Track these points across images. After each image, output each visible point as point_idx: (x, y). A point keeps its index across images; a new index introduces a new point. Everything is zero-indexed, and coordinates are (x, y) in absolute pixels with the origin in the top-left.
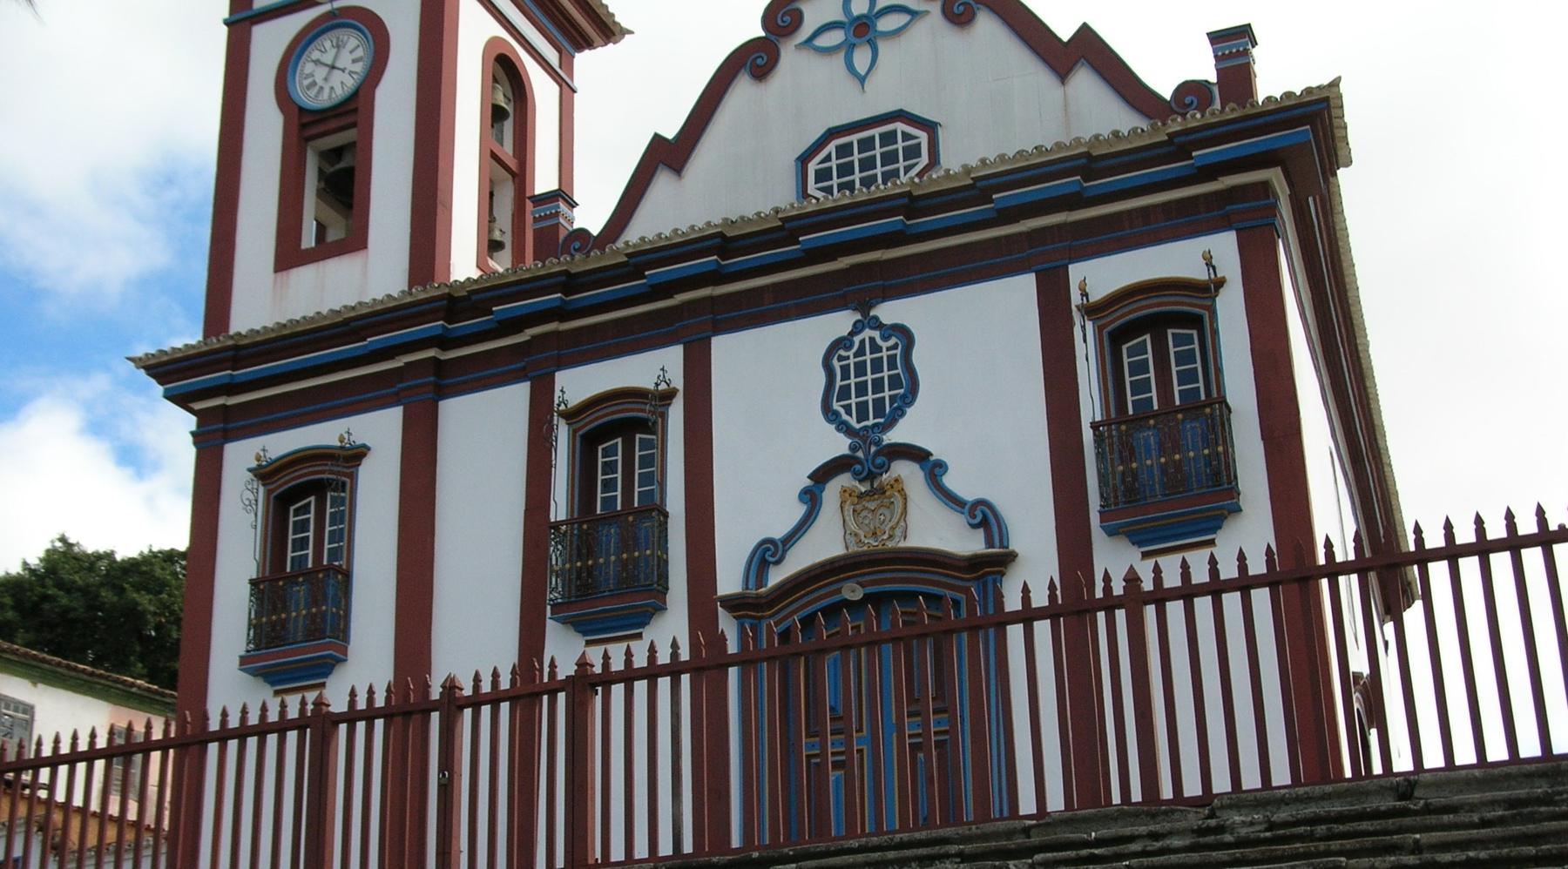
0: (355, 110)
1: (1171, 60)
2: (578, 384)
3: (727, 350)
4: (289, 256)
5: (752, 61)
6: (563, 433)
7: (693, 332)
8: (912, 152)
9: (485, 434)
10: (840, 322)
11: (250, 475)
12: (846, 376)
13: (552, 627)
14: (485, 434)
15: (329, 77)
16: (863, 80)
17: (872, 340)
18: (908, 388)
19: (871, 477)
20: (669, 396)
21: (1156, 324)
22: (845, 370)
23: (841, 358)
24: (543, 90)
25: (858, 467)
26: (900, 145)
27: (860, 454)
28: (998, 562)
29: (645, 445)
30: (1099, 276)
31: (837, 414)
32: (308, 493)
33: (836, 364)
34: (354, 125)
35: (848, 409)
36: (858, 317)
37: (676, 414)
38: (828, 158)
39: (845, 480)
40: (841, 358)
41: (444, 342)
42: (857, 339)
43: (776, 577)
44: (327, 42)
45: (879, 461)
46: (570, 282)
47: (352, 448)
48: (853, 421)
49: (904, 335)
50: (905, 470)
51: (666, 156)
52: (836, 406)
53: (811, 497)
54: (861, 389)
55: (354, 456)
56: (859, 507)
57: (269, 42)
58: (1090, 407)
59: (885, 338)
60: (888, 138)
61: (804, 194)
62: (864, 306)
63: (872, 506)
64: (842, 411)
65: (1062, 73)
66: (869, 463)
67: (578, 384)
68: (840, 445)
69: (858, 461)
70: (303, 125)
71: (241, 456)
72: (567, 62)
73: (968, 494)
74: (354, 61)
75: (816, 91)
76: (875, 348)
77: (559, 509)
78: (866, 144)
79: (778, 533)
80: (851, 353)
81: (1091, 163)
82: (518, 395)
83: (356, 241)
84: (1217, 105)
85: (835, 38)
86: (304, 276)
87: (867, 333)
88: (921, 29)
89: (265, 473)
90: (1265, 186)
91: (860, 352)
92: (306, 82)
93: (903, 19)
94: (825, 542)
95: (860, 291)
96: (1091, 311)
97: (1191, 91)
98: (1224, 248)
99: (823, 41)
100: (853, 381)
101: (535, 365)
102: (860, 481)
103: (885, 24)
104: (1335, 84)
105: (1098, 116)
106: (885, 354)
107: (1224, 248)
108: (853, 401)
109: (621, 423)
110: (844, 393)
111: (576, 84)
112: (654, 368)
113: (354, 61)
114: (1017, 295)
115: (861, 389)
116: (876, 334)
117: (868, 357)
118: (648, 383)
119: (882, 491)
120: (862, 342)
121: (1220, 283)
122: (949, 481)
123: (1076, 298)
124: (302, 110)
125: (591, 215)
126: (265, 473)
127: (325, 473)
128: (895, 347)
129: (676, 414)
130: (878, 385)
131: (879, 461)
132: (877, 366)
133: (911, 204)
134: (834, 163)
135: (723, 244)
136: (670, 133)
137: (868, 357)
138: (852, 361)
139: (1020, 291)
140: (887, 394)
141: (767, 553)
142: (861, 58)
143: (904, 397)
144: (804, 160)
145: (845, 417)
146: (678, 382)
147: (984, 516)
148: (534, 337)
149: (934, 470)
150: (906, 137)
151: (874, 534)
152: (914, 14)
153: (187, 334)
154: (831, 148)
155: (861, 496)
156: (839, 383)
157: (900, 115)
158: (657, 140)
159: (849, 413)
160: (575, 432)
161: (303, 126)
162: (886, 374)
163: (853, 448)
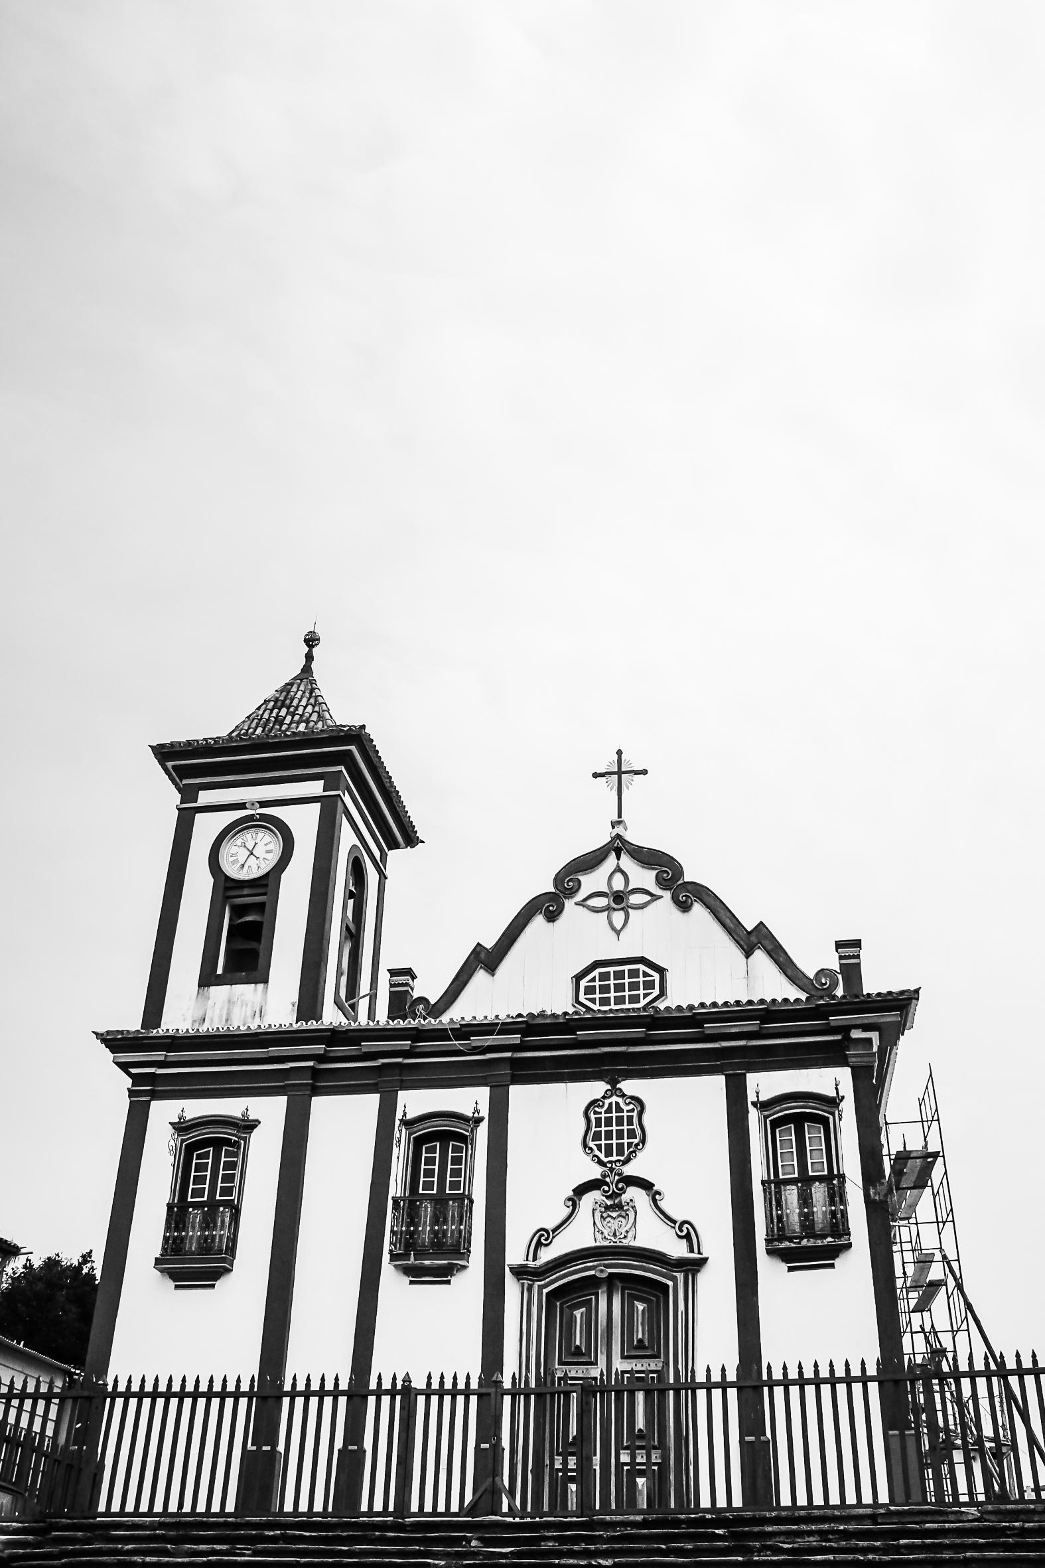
0: (268, 884)
1: (816, 956)
4: (208, 979)
5: (547, 906)
6: (401, 1135)
8: (649, 985)
10: (598, 1088)
11: (170, 1130)
12: (598, 1124)
15: (250, 857)
16: (618, 933)
17: (617, 1103)
20: (479, 1121)
22: (598, 1120)
23: (596, 1113)
25: (606, 1188)
26: (641, 979)
27: (607, 1179)
29: (457, 1149)
30: (765, 1084)
31: (591, 1149)
33: (593, 1117)
34: (265, 894)
35: (599, 1147)
36: (609, 1087)
37: (482, 1132)
38: (593, 980)
39: (595, 1196)
40: (596, 1113)
42: (607, 1102)
45: (620, 1185)
46: (418, 1035)
47: (248, 1120)
48: (602, 1156)
49: (638, 1101)
51: (487, 959)
52: (591, 1144)
54: (609, 1135)
55: (249, 1126)
56: (605, 1215)
57: (207, 828)
58: (758, 1172)
59: (628, 1104)
60: (634, 974)
62: (613, 1083)
63: (614, 1214)
64: (595, 1148)
66: (613, 1187)
67: (415, 1102)
68: (596, 1172)
69: (607, 1184)
73: (679, 1218)
74: (268, 852)
76: (619, 1109)
78: (619, 975)
79: (550, 1226)
80: (603, 1110)
86: (219, 993)
87: (614, 1099)
90: (869, 1041)
91: (609, 1110)
92: (231, 859)
93: (647, 898)
95: (610, 1067)
99: (591, 902)
100: (603, 1129)
101: (385, 1080)
102: (607, 1197)
103: (635, 899)
104: (917, 991)
106: (625, 1114)
108: (603, 1142)
109: (444, 1134)
110: (597, 1136)
111: (387, 873)
112: (470, 1100)
113: (268, 852)
114: (710, 1089)
115: (609, 1135)
116: (620, 1100)
117: (614, 1115)
119: (620, 1207)
120: (611, 1104)
123: (751, 1097)
124: (227, 878)
125: (429, 987)
128: (632, 1110)
129: (482, 1132)
130: (620, 1135)
131: (620, 1185)
132: (620, 1121)
134: (597, 983)
136: (489, 944)
137: (614, 1115)
138: (603, 1116)
139: (716, 1084)
140: (626, 1141)
141: (542, 1238)
143: (637, 1145)
144: (578, 978)
145: (597, 1153)
146: (484, 1112)
148: (384, 1064)
150: (645, 974)
151: (615, 1235)
154: (596, 973)
155: (607, 1208)
156: (594, 1129)
157: (642, 960)
158: (479, 944)
159: (600, 1150)
160: (410, 1135)
161: (227, 889)
162: (625, 1127)
163: (604, 1176)
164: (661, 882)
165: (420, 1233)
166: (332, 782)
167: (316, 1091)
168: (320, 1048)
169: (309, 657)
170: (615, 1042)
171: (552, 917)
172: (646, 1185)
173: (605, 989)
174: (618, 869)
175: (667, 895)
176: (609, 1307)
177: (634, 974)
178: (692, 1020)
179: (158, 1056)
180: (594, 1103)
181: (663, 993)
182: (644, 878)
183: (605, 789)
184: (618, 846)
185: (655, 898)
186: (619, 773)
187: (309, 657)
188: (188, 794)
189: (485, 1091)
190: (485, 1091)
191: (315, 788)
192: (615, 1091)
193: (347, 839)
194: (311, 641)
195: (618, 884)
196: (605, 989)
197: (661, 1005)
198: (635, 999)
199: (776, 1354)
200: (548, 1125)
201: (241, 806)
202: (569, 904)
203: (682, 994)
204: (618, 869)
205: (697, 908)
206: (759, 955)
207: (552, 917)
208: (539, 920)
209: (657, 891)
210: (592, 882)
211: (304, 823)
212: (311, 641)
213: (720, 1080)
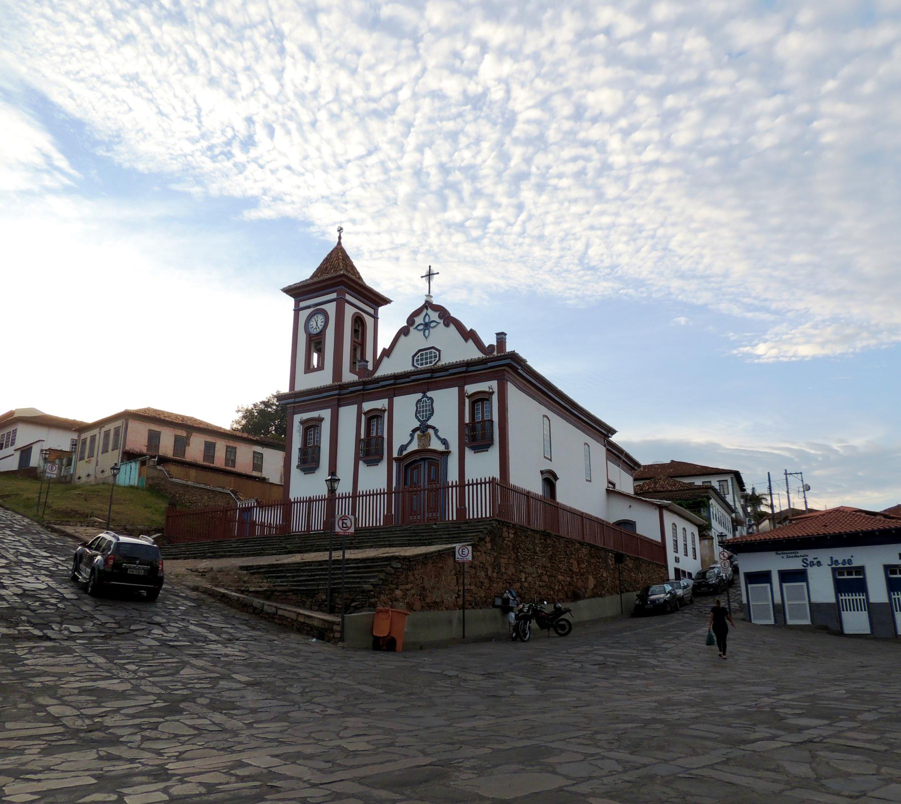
0: (322, 333)
3: (396, 399)
4: (308, 368)
5: (404, 332)
8: (435, 356)
9: (348, 415)
10: (419, 396)
13: (361, 462)
19: (424, 432)
20: (385, 411)
21: (482, 400)
24: (369, 321)
28: (446, 454)
30: (471, 389)
37: (386, 414)
39: (418, 432)
43: (405, 453)
49: (431, 399)
50: (431, 431)
53: (412, 436)
55: (321, 420)
60: (431, 353)
61: (413, 365)
62: (424, 393)
65: (466, 341)
66: (423, 429)
67: (367, 406)
68: (417, 424)
71: (297, 418)
75: (416, 341)
78: (426, 354)
79: (405, 443)
81: (469, 364)
82: (355, 407)
83: (321, 367)
84: (495, 353)
85: (421, 327)
88: (439, 326)
94: (414, 446)
96: (469, 397)
97: (491, 346)
99: (419, 328)
103: (433, 325)
107: (494, 384)
109: (374, 416)
112: (382, 404)
114: (455, 390)
121: (493, 393)
127: (314, 423)
129: (386, 414)
135: (396, 377)
141: (403, 448)
142: (427, 332)
147: (444, 442)
149: (436, 431)
152: (438, 323)
157: (433, 348)
158: (384, 349)
164: (440, 317)
165: (370, 450)
167: (339, 406)
168: (337, 392)
169: (340, 238)
170: (427, 378)
172: (433, 428)
173: (422, 359)
174: (427, 314)
175: (442, 321)
176: (424, 468)
177: (431, 353)
178: (445, 368)
179: (292, 400)
180: (419, 401)
181: (439, 359)
182: (434, 316)
183: (424, 282)
184: (428, 305)
186: (430, 275)
187: (340, 238)
189: (387, 400)
190: (387, 400)
191: (334, 296)
193: (349, 311)
194: (340, 230)
195: (427, 320)
197: (440, 364)
198: (431, 362)
199: (469, 476)
200: (405, 410)
202: (411, 329)
204: (427, 314)
205: (452, 326)
206: (470, 342)
209: (438, 320)
210: (419, 320)
211: (331, 309)
212: (340, 230)
213: (457, 388)
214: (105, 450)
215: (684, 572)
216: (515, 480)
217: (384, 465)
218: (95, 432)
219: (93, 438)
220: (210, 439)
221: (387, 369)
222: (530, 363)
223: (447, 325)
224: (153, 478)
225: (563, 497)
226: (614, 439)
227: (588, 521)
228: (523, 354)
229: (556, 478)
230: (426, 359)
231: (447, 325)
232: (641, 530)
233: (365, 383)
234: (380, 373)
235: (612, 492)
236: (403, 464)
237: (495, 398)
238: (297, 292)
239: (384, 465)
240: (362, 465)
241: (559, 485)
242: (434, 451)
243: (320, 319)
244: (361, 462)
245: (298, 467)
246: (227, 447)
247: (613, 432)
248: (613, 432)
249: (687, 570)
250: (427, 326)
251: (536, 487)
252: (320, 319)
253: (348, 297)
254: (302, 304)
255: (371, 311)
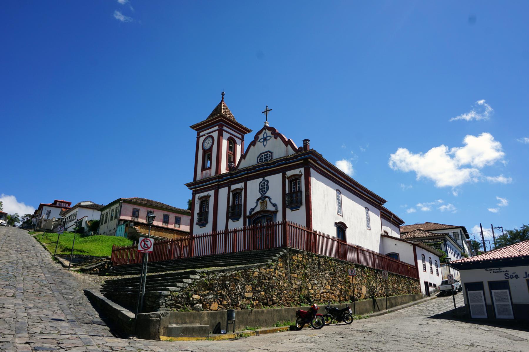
0: (211, 149)
2: (233, 187)
3: (249, 183)
4: (204, 168)
6: (231, 193)
7: (245, 180)
8: (270, 156)
10: (261, 179)
13: (230, 220)
14: (223, 192)
18: (268, 188)
28: (276, 212)
30: (289, 173)
32: (204, 201)
39: (260, 201)
41: (219, 182)
43: (253, 213)
44: (208, 140)
49: (267, 181)
50: (267, 199)
53: (257, 203)
55: (209, 197)
57: (202, 139)
60: (267, 154)
66: (263, 199)
68: (259, 196)
70: (205, 151)
71: (197, 196)
72: (243, 137)
73: (273, 203)
77: (230, 205)
78: (265, 155)
81: (286, 160)
82: (226, 189)
83: (210, 168)
86: (204, 172)
89: (200, 199)
94: (258, 209)
95: (263, 175)
98: (302, 170)
101: (229, 185)
103: (268, 138)
105: (291, 152)
107: (302, 170)
112: (241, 185)
118: (239, 187)
121: (302, 175)
122: (272, 201)
126: (200, 199)
133: (267, 165)
135: (248, 170)
141: (252, 210)
142: (265, 143)
147: (275, 205)
152: (271, 137)
153: (191, 180)
157: (268, 151)
164: (272, 134)
165: (234, 212)
166: (221, 126)
169: (223, 98)
171: (254, 146)
172: (269, 197)
174: (265, 133)
175: (273, 136)
177: (267, 154)
180: (261, 182)
182: (269, 133)
184: (265, 128)
185: (271, 137)
187: (223, 98)
188: (198, 134)
191: (217, 128)
192: (264, 179)
196: (262, 159)
198: (267, 160)
201: (204, 135)
203: (276, 156)
205: (279, 138)
207: (254, 146)
208: (252, 147)
210: (261, 136)
211: (215, 135)
212: (223, 94)
214: (112, 219)
215: (431, 284)
216: (316, 227)
217: (242, 220)
218: (108, 210)
219: (107, 214)
220: (166, 213)
221: (245, 164)
222: (325, 157)
223: (276, 138)
224: (131, 233)
225: (351, 238)
226: (385, 206)
227: (362, 252)
228: (319, 151)
229: (346, 227)
230: (265, 158)
231: (276, 138)
232: (402, 259)
233: (231, 174)
234: (241, 167)
235: (385, 236)
236: (252, 220)
237: (303, 178)
238: (199, 128)
239: (242, 220)
240: (230, 221)
241: (348, 232)
242: (269, 211)
243: (210, 141)
244: (230, 220)
245: (197, 224)
246: (176, 217)
247: (384, 202)
248: (384, 202)
249: (433, 283)
250: (265, 139)
251: (333, 232)
252: (210, 141)
253: (225, 128)
254: (201, 134)
255: (240, 136)
